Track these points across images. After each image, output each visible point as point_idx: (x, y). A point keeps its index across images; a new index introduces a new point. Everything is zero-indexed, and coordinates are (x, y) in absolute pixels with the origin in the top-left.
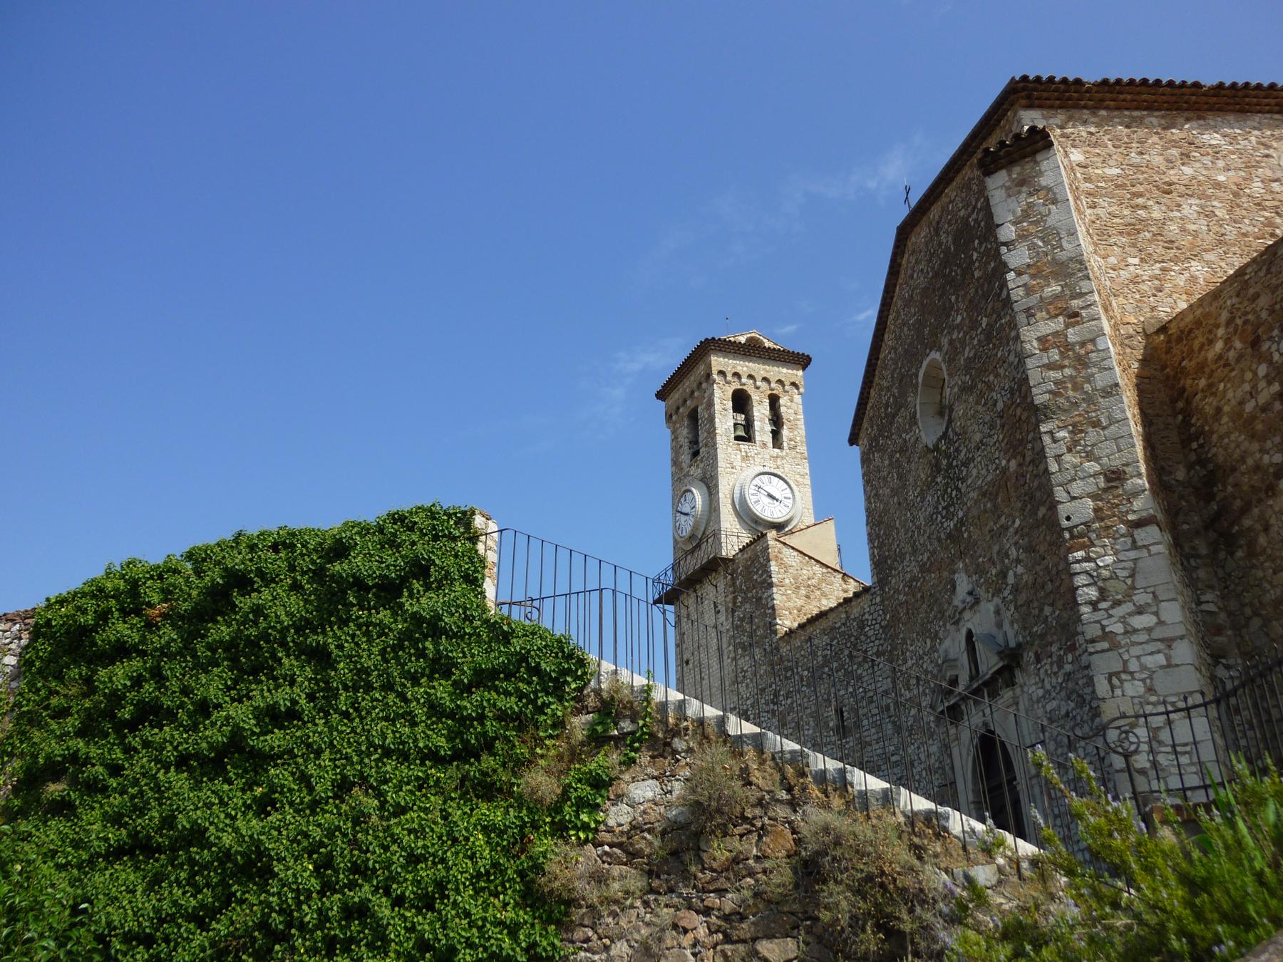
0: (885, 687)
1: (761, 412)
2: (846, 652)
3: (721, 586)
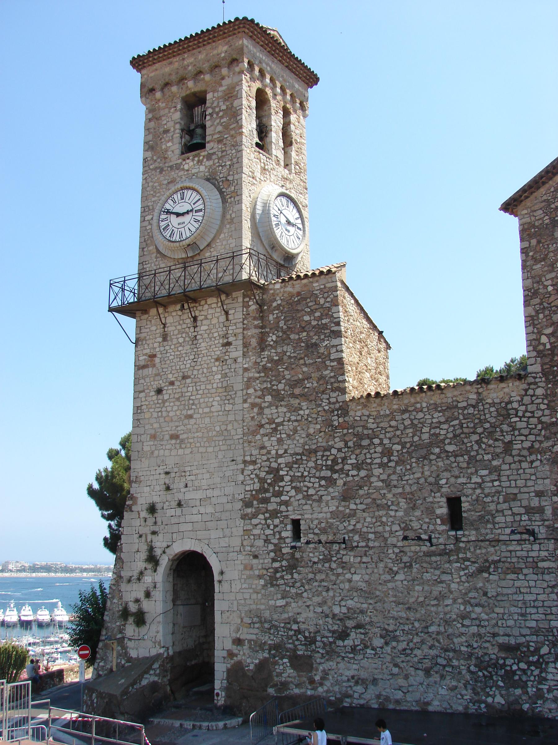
0: (541, 488)
1: (276, 122)
2: (475, 437)
3: (237, 314)
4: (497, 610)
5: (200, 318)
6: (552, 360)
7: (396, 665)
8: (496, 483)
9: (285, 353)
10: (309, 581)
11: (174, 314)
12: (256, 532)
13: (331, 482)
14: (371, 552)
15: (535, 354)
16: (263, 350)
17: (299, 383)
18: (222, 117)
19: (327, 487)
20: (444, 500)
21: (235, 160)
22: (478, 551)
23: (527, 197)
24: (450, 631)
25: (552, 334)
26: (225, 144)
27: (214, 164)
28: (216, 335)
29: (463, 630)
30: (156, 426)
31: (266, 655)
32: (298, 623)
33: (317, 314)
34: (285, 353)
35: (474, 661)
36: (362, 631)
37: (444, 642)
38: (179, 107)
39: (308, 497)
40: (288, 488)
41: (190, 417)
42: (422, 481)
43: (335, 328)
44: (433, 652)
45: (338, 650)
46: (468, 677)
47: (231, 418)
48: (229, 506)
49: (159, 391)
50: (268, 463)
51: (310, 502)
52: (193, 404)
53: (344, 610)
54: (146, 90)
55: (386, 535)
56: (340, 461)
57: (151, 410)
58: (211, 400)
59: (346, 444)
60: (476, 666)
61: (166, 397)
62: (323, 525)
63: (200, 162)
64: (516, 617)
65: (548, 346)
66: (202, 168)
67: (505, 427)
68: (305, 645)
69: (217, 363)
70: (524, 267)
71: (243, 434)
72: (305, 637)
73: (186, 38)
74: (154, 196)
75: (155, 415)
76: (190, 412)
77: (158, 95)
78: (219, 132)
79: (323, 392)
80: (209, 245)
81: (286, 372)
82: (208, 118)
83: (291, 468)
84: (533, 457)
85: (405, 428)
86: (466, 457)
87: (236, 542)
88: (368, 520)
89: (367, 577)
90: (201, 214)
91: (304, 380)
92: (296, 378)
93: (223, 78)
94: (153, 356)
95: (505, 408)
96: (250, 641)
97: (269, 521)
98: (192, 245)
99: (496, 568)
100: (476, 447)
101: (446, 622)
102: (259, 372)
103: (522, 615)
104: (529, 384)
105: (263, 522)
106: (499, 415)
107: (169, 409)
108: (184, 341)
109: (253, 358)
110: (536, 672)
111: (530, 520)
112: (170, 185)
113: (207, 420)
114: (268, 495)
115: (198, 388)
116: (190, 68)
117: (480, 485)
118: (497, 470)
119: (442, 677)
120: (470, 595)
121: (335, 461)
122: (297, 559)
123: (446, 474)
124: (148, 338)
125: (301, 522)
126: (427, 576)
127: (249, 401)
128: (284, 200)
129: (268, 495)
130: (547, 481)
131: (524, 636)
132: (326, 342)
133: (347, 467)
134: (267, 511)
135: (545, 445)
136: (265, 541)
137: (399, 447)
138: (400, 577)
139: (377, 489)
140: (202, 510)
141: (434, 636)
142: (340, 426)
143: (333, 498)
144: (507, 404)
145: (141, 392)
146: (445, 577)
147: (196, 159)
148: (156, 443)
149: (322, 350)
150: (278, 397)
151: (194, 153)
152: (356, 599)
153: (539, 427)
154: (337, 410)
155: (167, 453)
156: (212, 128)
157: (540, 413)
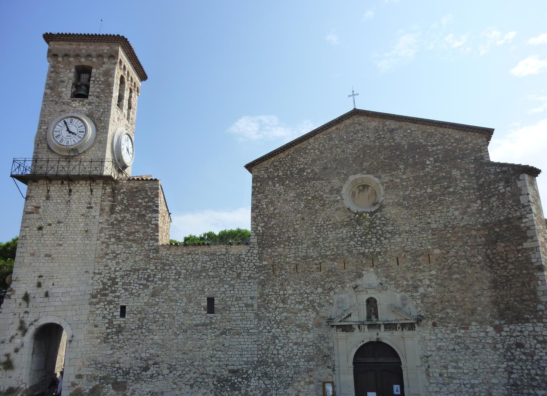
0: (253, 295)
1: (126, 95)
2: (223, 269)
4: (229, 353)
5: (73, 191)
6: (262, 238)
7: (175, 384)
8: (232, 292)
9: (125, 217)
10: (128, 340)
11: (56, 185)
12: (98, 312)
13: (146, 286)
14: (165, 324)
15: (255, 234)
16: (112, 213)
17: (132, 233)
18: (100, 84)
19: (143, 289)
20: (206, 298)
21: (106, 110)
22: (221, 324)
23: (257, 164)
24: (205, 364)
25: (264, 226)
26: (101, 100)
27: (93, 108)
28: (83, 201)
29: (211, 363)
30: (35, 248)
31: (98, 383)
32: (119, 363)
33: (146, 200)
34: (125, 217)
35: (216, 379)
36: (157, 366)
37: (201, 370)
38: (73, 70)
39: (132, 294)
40: (121, 289)
41: (61, 245)
42: (195, 289)
43: (156, 208)
44: (194, 376)
45: (142, 377)
46: (212, 387)
47: (88, 248)
48: (82, 297)
49: (40, 228)
50: (109, 275)
51: (133, 297)
52: (63, 238)
53: (148, 355)
54: (51, 54)
55: (175, 315)
56: (152, 276)
57: (33, 239)
58: (76, 237)
59: (156, 268)
60: (217, 381)
61: (45, 232)
62: (139, 309)
63: (83, 105)
64: (238, 356)
65: (261, 232)
66: (85, 109)
67: (238, 266)
68: (123, 375)
69: (82, 217)
70: (253, 195)
71: (95, 258)
72: (123, 371)
73: (85, 34)
74: (49, 116)
75: (36, 242)
76: (60, 242)
77: (60, 59)
78: (98, 92)
79: (146, 240)
80: (84, 152)
81: (125, 227)
82: (91, 82)
83: (123, 278)
84: (250, 281)
85: (189, 262)
86: (218, 278)
87: (84, 318)
88: (165, 307)
89: (162, 337)
90: (83, 134)
91: (135, 232)
92: (131, 231)
93: (104, 63)
94: (37, 208)
95: (239, 257)
96: (87, 375)
97: (107, 306)
98: (75, 150)
99: (230, 332)
100: (223, 274)
101: (203, 359)
102: (109, 225)
103: (241, 355)
104: (251, 247)
105: (103, 307)
106: (236, 260)
107: (46, 239)
108: (61, 202)
109: (106, 217)
110: (246, 382)
111: (247, 310)
112: (62, 113)
113: (72, 248)
114: (107, 292)
115: (68, 229)
116: (83, 51)
117: (224, 292)
118: (233, 286)
119: (199, 388)
120: (217, 345)
121: (149, 276)
122: (122, 328)
123: (207, 286)
124: (35, 196)
125: (127, 307)
126: (195, 336)
127: (101, 240)
128: (127, 136)
129: (107, 292)
130: (256, 292)
131: (241, 365)
132: (150, 215)
133: (155, 279)
134: (106, 301)
135: (256, 275)
136: (103, 317)
137: (185, 271)
138: (181, 337)
139: (172, 292)
140: (63, 299)
141: (196, 367)
142: (153, 258)
143: (146, 295)
144: (240, 255)
145: (26, 227)
146: (204, 337)
147: (81, 103)
148: (34, 258)
149: (147, 218)
150: (119, 239)
151: (80, 99)
152: (155, 349)
153: (254, 267)
154: (153, 250)
155: (41, 264)
156: (94, 89)
157: (255, 261)
